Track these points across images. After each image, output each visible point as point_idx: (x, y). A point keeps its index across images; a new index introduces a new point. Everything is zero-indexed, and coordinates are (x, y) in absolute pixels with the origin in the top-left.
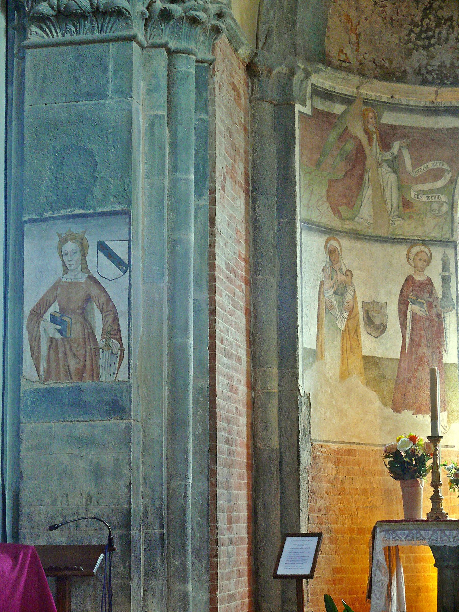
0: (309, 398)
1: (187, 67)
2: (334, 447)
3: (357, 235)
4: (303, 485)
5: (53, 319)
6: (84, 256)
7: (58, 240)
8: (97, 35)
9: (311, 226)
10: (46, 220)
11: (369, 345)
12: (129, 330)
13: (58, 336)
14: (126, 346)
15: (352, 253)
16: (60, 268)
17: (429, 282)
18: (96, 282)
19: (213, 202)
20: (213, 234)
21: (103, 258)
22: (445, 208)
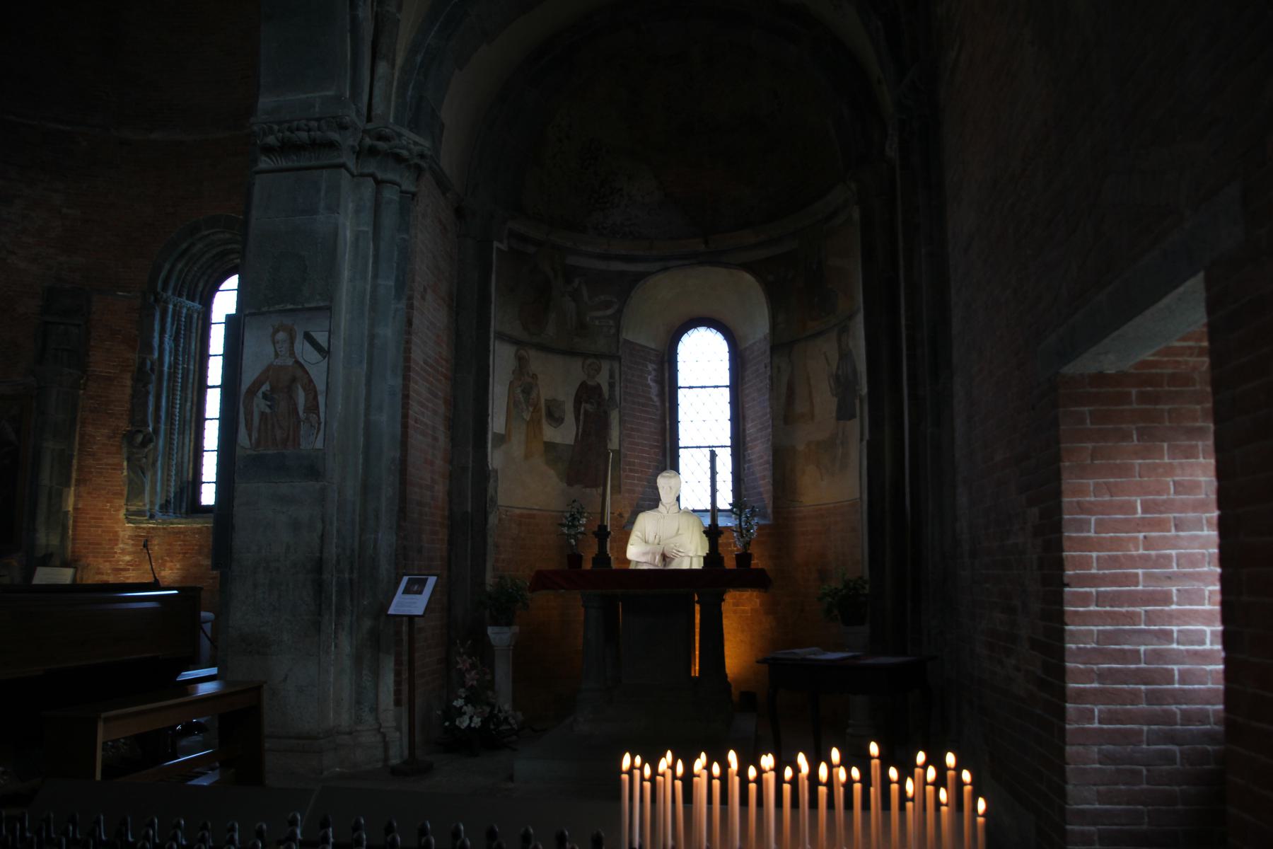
0: (496, 472)
1: (390, 194)
2: (518, 512)
3: (542, 348)
4: (490, 540)
5: (265, 396)
6: (292, 343)
7: (271, 330)
8: (313, 163)
9: (501, 337)
10: (263, 314)
11: (550, 433)
12: (326, 405)
13: (268, 410)
14: (322, 420)
15: (538, 363)
16: (272, 356)
17: (599, 387)
18: (301, 365)
19: (411, 307)
20: (409, 333)
21: (307, 345)
22: (613, 331)
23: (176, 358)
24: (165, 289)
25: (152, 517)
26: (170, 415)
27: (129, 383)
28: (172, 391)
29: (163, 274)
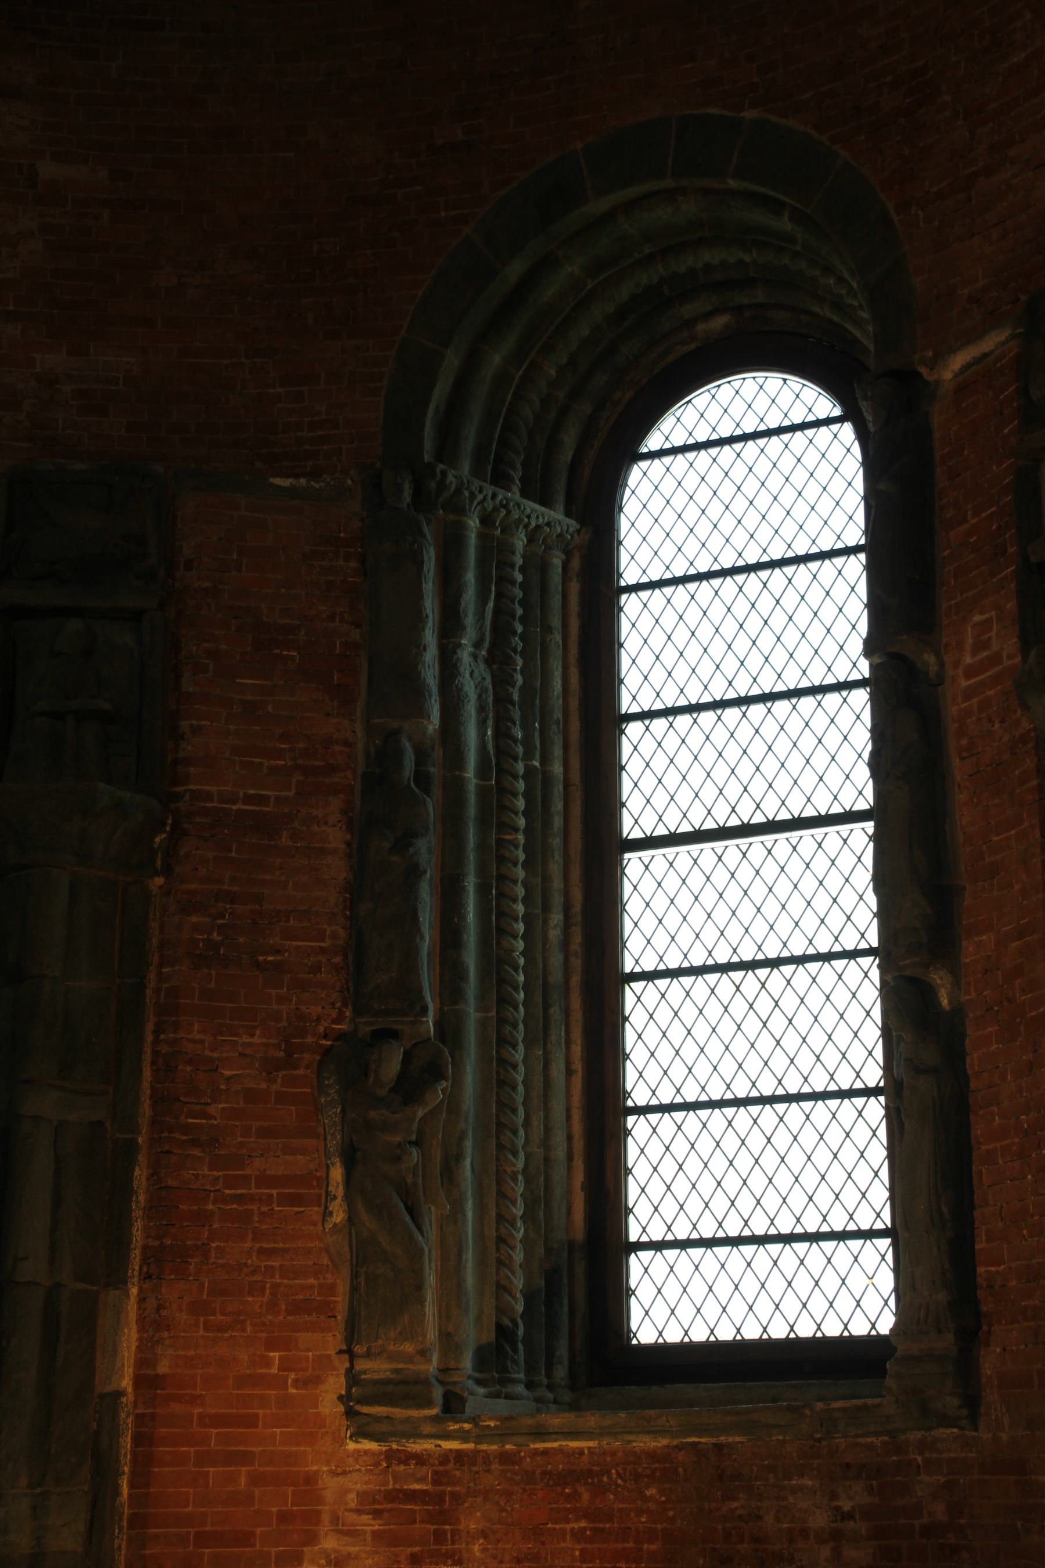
23: (502, 734)
24: (446, 451)
25: (453, 1405)
26: (496, 965)
27: (336, 837)
28: (495, 856)
29: (441, 391)
